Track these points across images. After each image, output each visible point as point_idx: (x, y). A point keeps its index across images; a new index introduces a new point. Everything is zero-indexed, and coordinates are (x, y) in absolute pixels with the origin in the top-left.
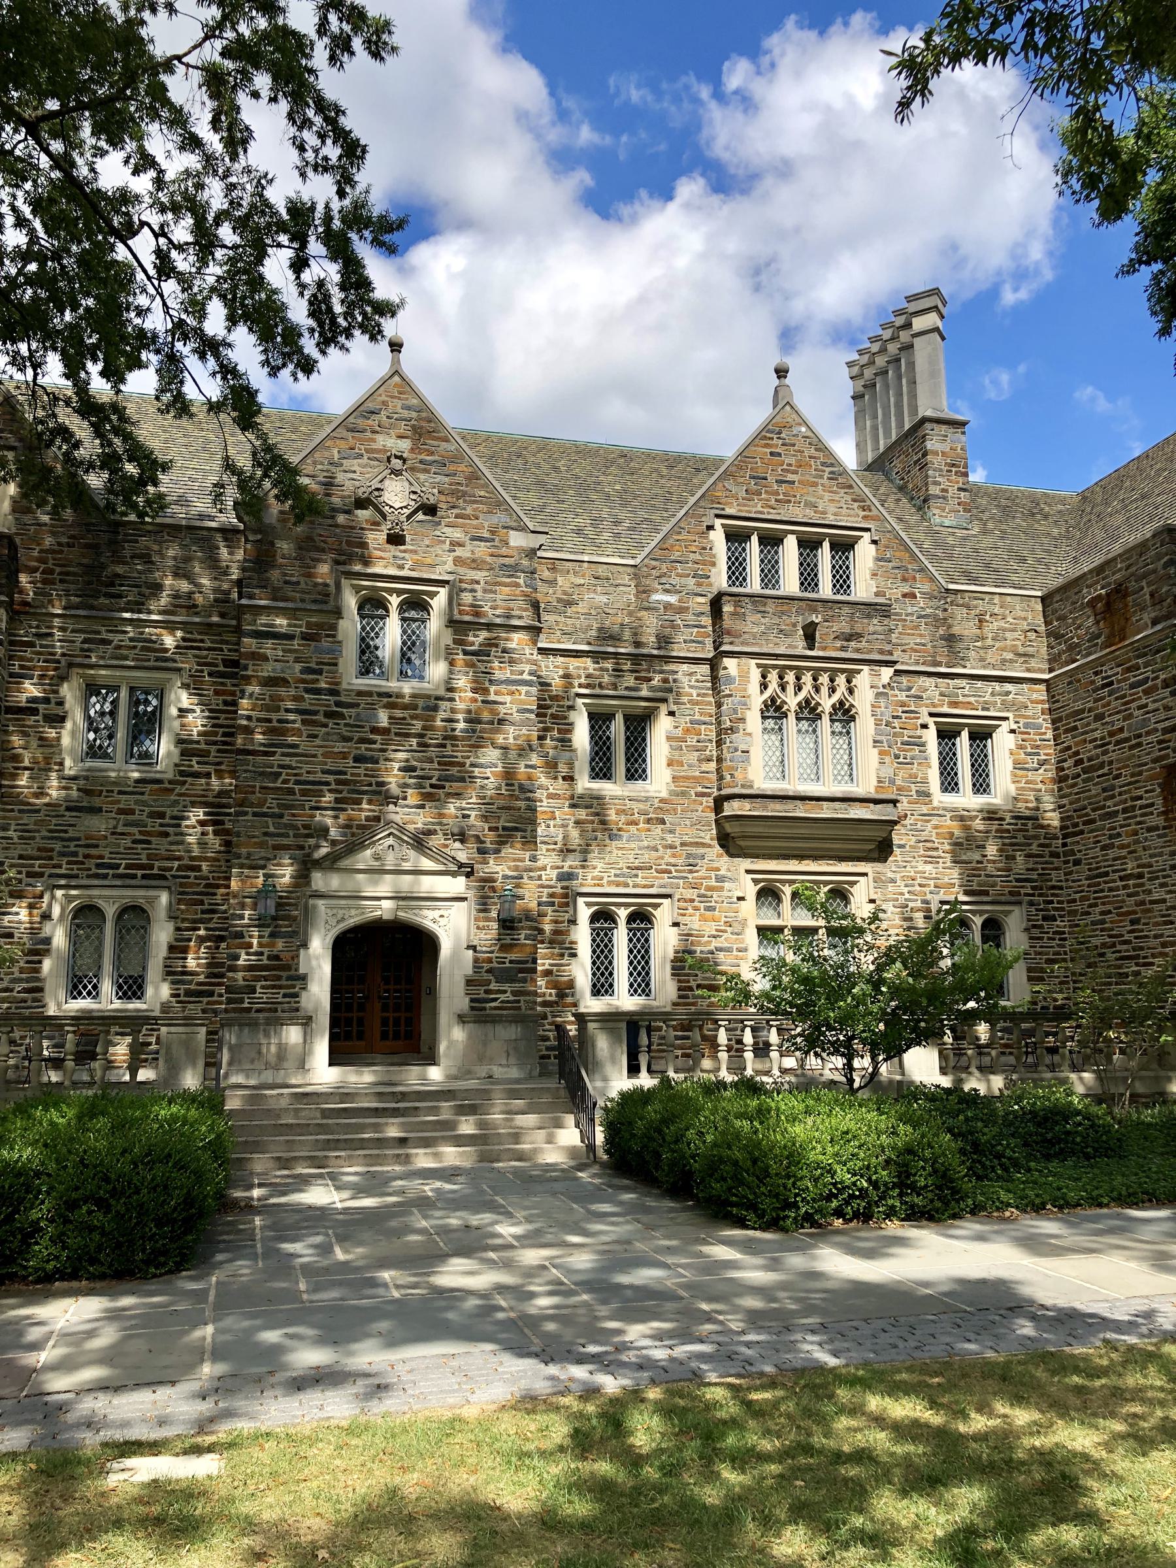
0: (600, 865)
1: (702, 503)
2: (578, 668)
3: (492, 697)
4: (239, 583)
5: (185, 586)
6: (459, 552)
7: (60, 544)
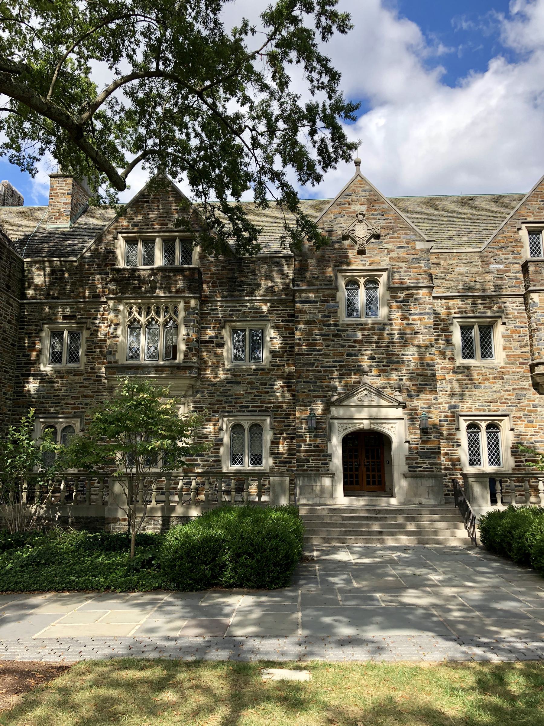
0: (470, 401)
1: (514, 217)
2: (454, 304)
3: (411, 322)
4: (293, 280)
5: (270, 283)
6: (392, 255)
7: (218, 270)
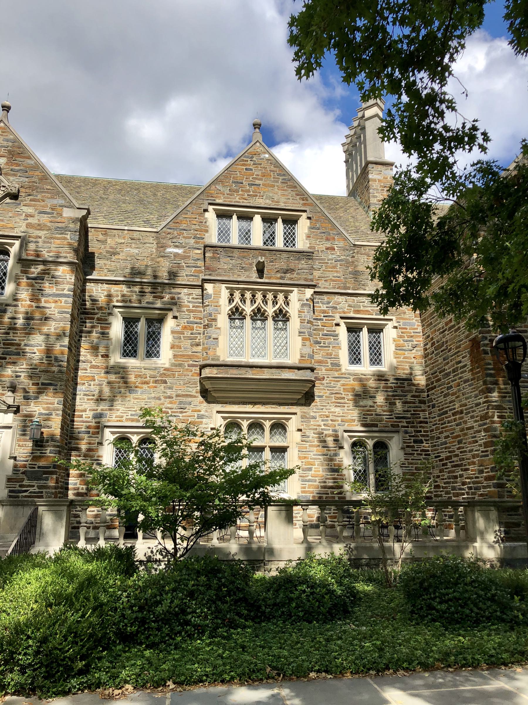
0: (121, 409)
1: (201, 197)
2: (117, 291)
3: (43, 304)
6: (30, 220)
